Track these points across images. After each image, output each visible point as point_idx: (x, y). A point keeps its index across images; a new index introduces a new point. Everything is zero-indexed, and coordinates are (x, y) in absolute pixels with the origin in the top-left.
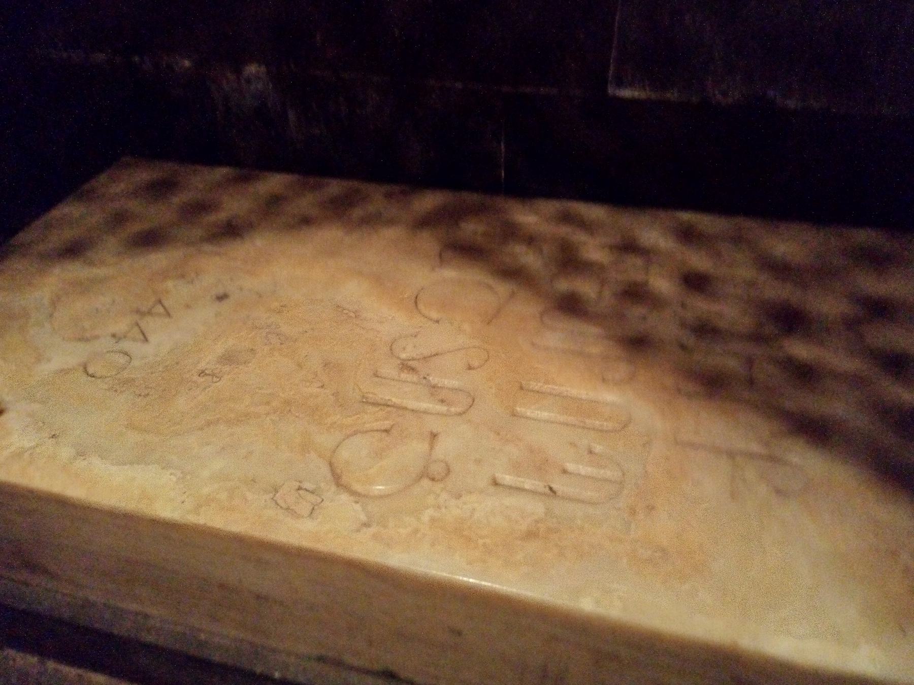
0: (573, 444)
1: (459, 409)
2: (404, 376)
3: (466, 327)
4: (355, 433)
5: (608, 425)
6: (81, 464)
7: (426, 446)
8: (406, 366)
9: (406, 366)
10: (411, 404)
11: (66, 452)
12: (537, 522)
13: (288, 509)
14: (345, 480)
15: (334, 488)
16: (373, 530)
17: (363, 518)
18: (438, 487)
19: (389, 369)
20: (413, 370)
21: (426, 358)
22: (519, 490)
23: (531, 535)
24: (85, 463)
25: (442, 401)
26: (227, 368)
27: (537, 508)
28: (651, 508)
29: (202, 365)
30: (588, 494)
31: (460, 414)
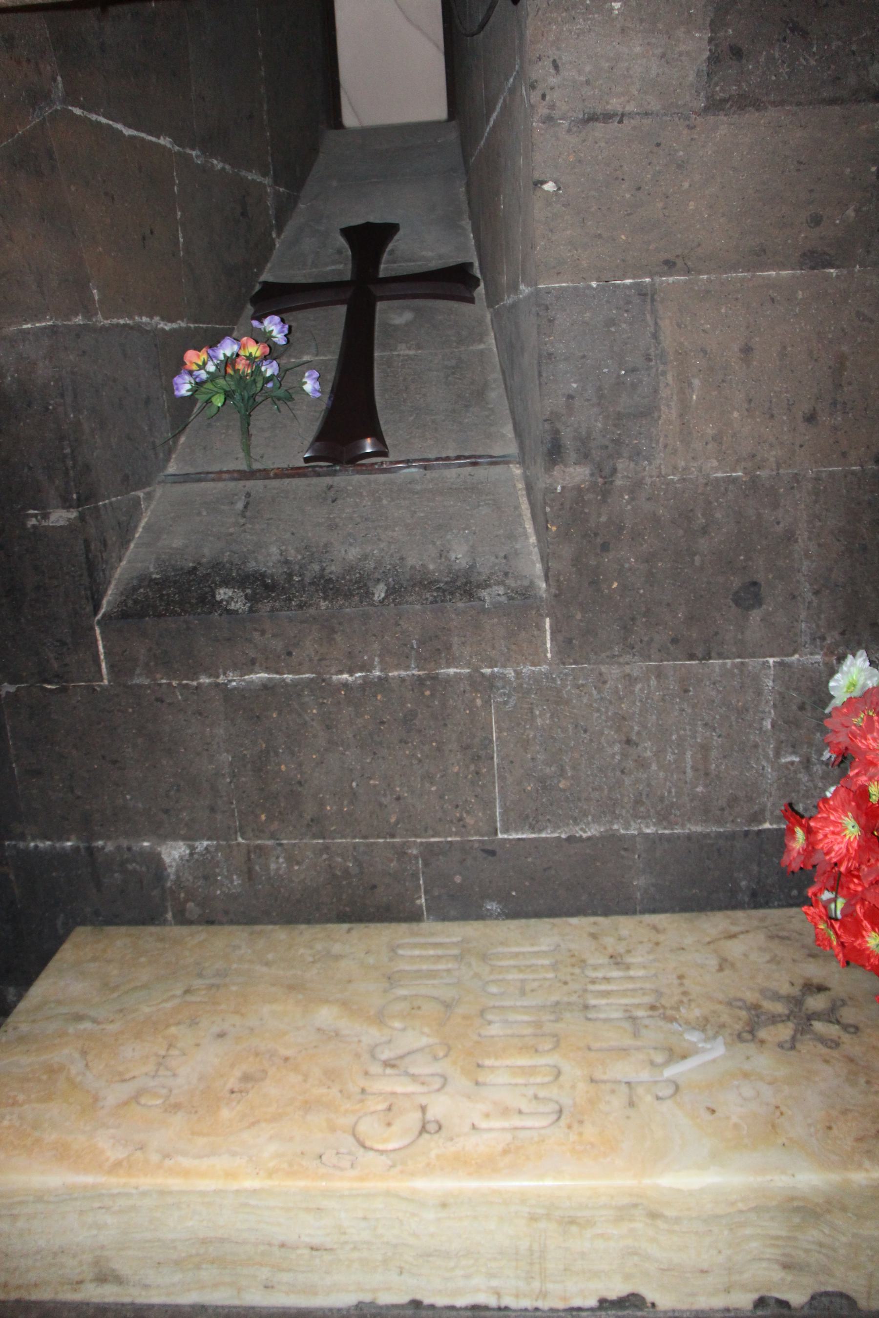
0: (524, 1096)
1: (437, 1086)
2: (389, 1071)
3: (426, 1030)
4: (366, 1114)
5: (547, 1079)
6: (168, 1163)
7: (418, 1115)
8: (387, 1064)
9: (387, 1064)
10: (399, 1089)
11: (155, 1158)
12: (508, 1144)
13: (334, 1166)
14: (368, 1143)
15: (362, 1150)
16: (399, 1168)
17: (389, 1163)
18: (436, 1136)
19: (376, 1069)
20: (393, 1066)
21: (402, 1057)
22: (491, 1130)
23: (505, 1152)
24: (172, 1162)
25: (423, 1083)
26: (250, 1085)
27: (508, 1137)
28: (581, 1122)
29: (229, 1086)
30: (537, 1124)
31: (438, 1090)
